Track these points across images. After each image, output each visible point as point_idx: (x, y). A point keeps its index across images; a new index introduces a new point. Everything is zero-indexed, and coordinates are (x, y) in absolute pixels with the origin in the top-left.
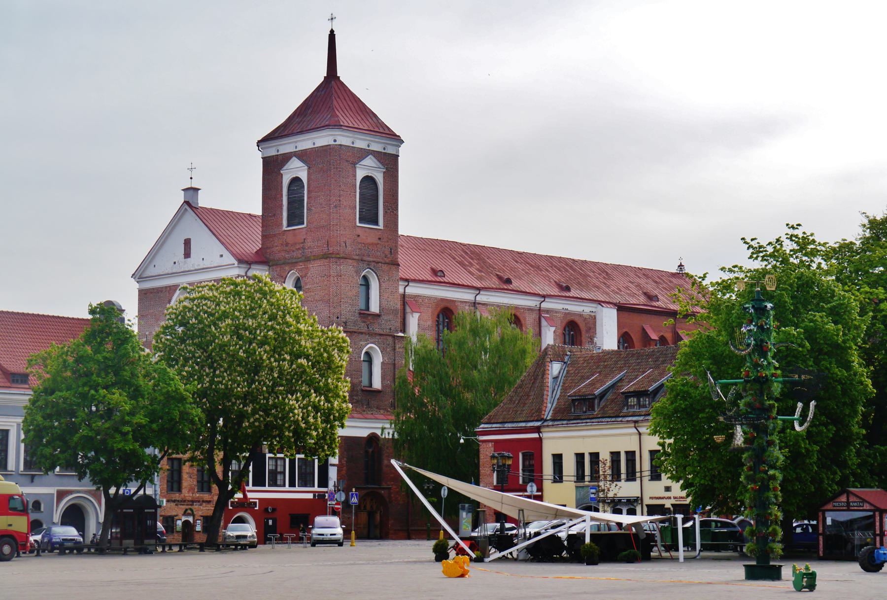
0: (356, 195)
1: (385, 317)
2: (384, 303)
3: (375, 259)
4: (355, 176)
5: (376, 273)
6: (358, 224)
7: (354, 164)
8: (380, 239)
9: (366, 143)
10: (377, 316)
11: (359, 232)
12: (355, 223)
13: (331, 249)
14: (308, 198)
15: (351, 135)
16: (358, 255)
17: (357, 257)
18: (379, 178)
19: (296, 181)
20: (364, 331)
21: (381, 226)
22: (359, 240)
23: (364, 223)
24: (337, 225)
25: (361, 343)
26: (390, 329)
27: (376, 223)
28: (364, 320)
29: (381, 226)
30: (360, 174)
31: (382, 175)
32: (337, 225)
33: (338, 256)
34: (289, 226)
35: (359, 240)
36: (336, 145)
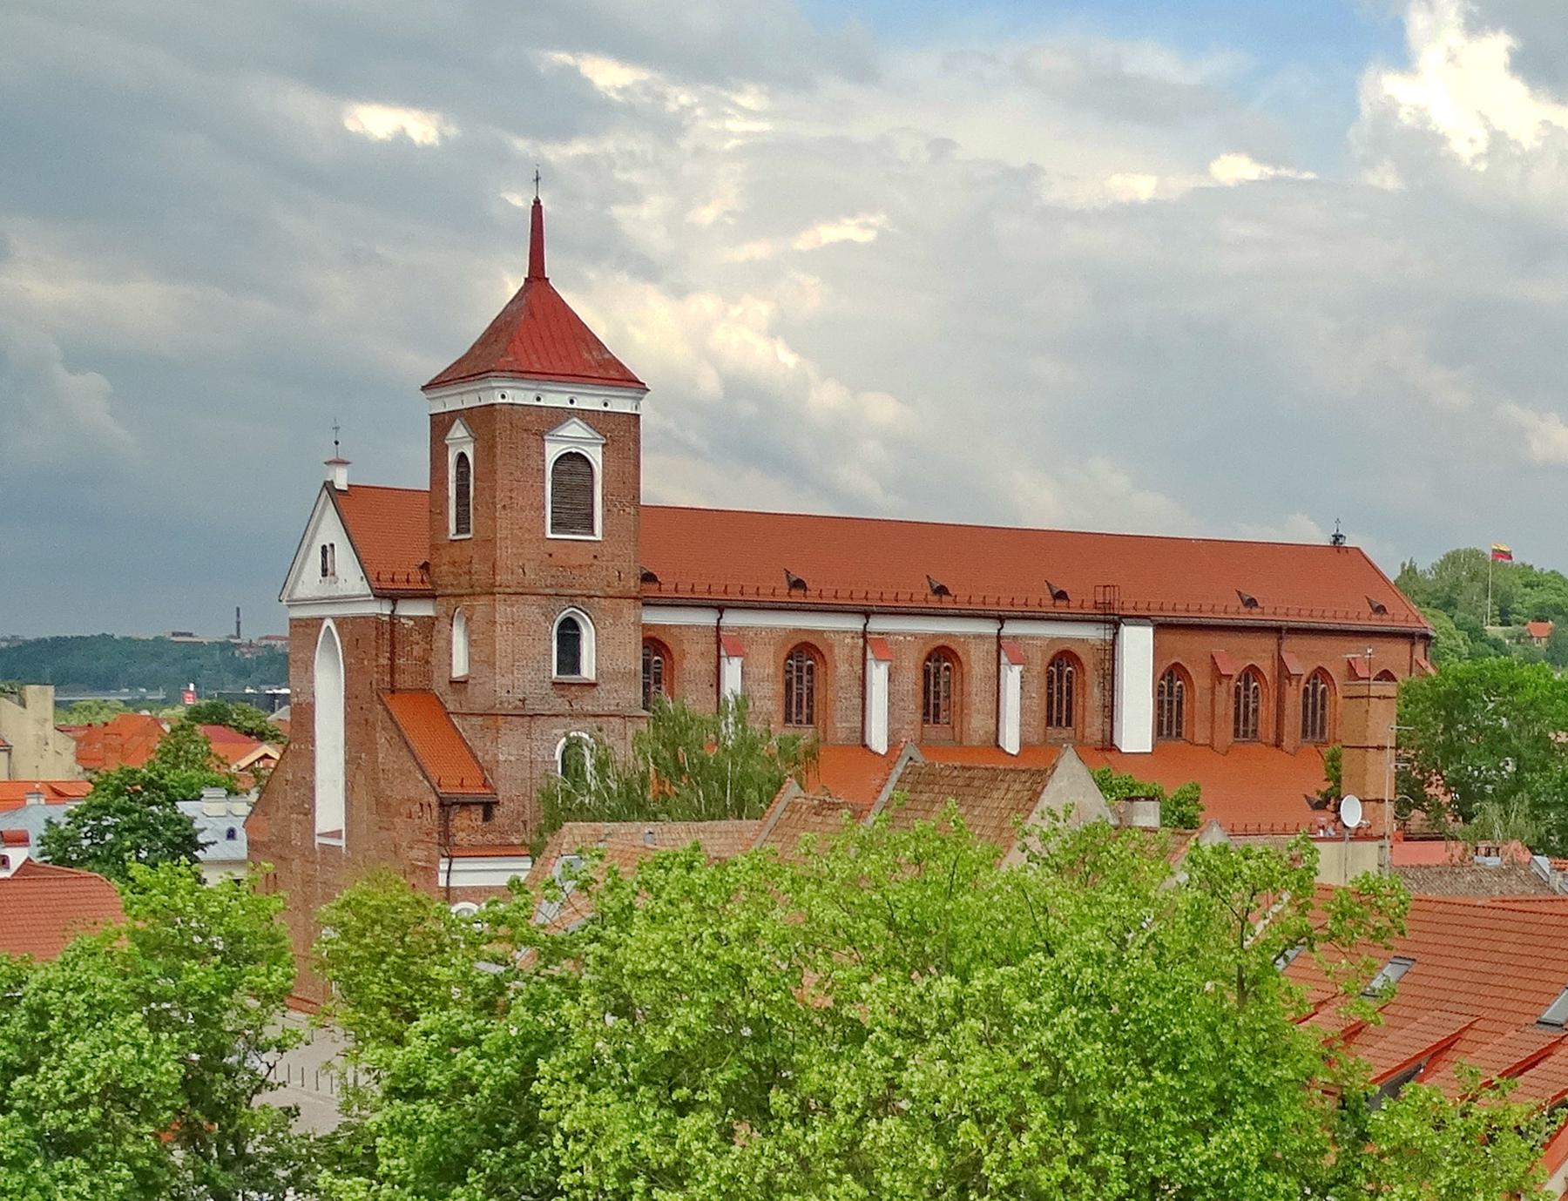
0: (543, 488)
1: (601, 693)
2: (605, 664)
3: (585, 592)
4: (543, 454)
5: (587, 614)
6: (550, 535)
7: (541, 436)
8: (595, 557)
9: (567, 397)
10: (594, 685)
11: (552, 548)
12: (544, 534)
13: (498, 578)
14: (475, 489)
15: (534, 387)
16: (552, 586)
17: (548, 591)
18: (595, 455)
19: (462, 457)
20: (561, 709)
21: (598, 535)
22: (552, 561)
23: (563, 533)
24: (506, 538)
25: (555, 731)
26: (618, 705)
27: (593, 534)
28: (562, 692)
29: (598, 535)
30: (553, 451)
31: (600, 448)
32: (506, 538)
33: (508, 590)
34: (458, 531)
35: (552, 561)
36: (505, 404)
